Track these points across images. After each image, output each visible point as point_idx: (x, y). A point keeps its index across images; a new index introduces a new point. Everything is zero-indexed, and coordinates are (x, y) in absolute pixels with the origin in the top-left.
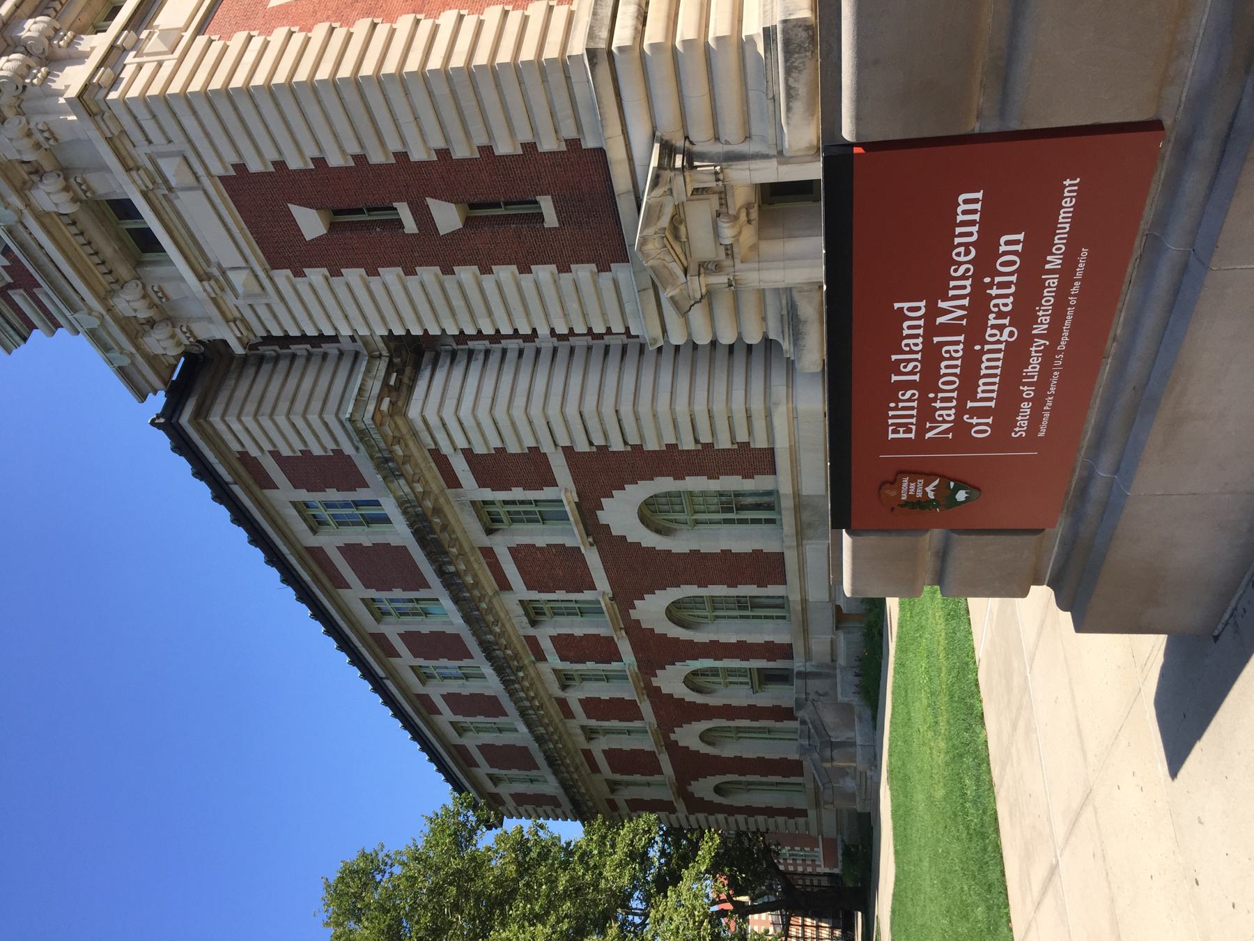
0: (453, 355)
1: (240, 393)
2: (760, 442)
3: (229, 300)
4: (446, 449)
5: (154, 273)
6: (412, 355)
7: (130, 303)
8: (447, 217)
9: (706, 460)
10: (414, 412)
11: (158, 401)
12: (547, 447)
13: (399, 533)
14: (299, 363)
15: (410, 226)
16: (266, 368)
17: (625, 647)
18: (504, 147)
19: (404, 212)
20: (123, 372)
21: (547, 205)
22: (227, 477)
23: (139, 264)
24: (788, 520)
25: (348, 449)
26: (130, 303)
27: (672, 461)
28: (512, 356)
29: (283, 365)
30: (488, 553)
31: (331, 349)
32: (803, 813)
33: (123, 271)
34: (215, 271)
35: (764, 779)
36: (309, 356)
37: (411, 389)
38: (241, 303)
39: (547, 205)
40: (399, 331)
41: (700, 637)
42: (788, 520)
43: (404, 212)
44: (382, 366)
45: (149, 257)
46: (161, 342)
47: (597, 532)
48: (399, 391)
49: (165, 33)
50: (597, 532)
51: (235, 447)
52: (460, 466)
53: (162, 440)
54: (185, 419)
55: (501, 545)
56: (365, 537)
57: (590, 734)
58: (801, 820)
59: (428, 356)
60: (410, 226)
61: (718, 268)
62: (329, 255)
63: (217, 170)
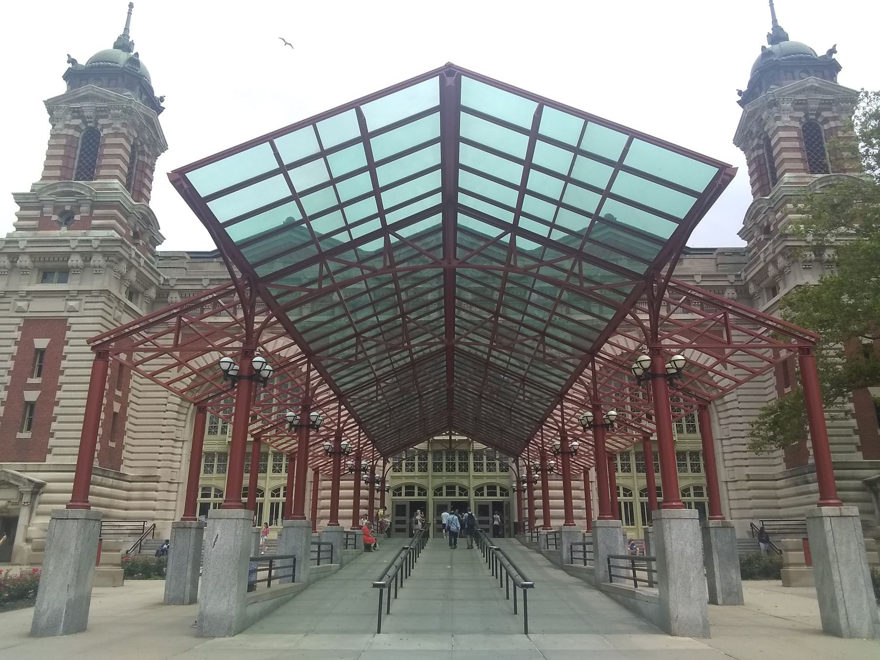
3: (15, 297)
5: (35, 276)
8: (31, 396)
15: (30, 381)
18: (54, 425)
19: (38, 380)
21: (26, 435)
23: (40, 270)
33: (38, 264)
34: (28, 298)
39: (26, 435)
43: (38, 380)
45: (41, 275)
49: (120, 317)
60: (30, 381)
62: (24, 344)
63: (71, 320)
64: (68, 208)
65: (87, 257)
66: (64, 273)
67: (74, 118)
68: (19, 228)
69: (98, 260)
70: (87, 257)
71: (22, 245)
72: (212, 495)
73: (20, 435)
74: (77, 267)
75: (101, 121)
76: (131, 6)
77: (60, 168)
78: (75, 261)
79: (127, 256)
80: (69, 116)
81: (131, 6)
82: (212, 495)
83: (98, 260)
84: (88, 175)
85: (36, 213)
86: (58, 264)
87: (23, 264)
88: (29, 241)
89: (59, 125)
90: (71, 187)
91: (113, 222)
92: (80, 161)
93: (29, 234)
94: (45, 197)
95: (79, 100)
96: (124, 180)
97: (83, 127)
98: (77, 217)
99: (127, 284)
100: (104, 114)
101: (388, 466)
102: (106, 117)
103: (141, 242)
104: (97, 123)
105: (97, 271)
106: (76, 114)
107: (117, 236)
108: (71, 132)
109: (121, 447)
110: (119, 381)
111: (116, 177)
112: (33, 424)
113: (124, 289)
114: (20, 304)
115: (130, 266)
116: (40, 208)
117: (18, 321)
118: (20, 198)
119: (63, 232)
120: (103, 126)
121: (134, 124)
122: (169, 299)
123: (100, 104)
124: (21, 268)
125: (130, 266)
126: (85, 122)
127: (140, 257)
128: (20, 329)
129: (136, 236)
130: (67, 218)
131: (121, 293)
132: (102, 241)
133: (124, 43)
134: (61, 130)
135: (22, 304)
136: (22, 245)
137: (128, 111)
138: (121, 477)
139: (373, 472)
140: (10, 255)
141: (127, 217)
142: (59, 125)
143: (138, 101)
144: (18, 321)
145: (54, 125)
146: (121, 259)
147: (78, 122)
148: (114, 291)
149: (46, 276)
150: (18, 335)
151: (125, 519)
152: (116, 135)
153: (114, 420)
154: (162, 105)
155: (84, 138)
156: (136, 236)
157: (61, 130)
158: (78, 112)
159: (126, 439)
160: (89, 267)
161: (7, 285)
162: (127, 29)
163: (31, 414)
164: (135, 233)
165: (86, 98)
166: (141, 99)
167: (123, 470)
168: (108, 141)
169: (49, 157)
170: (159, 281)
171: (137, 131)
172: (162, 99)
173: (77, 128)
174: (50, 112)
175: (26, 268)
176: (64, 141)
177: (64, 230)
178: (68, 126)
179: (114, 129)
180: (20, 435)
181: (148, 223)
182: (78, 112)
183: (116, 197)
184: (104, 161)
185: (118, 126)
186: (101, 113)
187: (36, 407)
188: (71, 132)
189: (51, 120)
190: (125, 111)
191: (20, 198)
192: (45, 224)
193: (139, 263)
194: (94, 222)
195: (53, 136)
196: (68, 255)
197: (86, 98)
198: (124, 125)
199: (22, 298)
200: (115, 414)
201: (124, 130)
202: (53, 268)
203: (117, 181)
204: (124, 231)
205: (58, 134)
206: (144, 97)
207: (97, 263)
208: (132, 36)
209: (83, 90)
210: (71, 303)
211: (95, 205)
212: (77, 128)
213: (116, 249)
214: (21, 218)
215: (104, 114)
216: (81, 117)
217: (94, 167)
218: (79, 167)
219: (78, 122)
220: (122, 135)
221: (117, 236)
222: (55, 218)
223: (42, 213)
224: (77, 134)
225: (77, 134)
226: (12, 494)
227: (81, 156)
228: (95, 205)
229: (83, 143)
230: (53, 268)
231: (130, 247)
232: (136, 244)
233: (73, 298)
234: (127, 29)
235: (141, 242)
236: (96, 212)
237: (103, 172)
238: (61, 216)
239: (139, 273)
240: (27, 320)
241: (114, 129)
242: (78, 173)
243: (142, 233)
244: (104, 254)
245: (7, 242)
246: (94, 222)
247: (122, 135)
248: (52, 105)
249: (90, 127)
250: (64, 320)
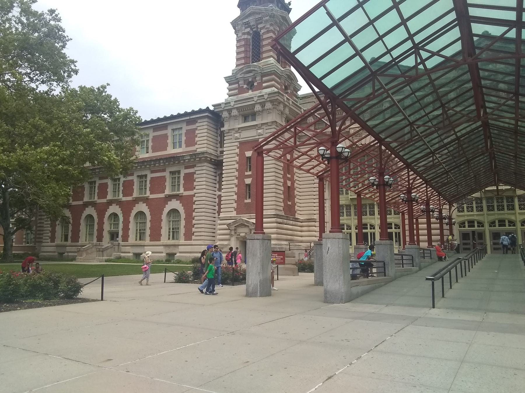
0: (216, 173)
1: (212, 125)
2: (193, 237)
3: (233, 132)
4: (196, 169)
5: (241, 119)
6: (218, 165)
7: (235, 112)
9: (189, 225)
10: (206, 164)
11: (212, 108)
12: (195, 191)
13: (171, 151)
14: (215, 138)
15: (246, 173)
16: (215, 131)
17: (129, 198)
19: (249, 173)
20: (219, 105)
22: (191, 117)
23: (242, 116)
24: (171, 242)
25: (197, 146)
26: (235, 112)
27: (189, 218)
28: (215, 185)
29: (216, 135)
30: (164, 170)
31: (219, 145)
32: (53, 240)
33: (241, 113)
34: (240, 131)
35: (70, 231)
36: (217, 140)
37: (210, 163)
38: (232, 134)
40: (224, 164)
41: (132, 219)
42: (171, 242)
43: (249, 173)
44: (216, 159)
46: (225, 115)
47: (170, 198)
48: (210, 162)
50: (170, 198)
51: (199, 121)
52: (191, 170)
53: (204, 108)
54: (207, 114)
55: (167, 174)
56: (170, 141)
57: (92, 183)
58: (49, 241)
59: (216, 167)
60: (246, 173)
61: (235, 233)
62: (241, 155)
64: (250, 80)
65: (263, 104)
66: (253, 115)
67: (246, 28)
68: (230, 96)
69: (268, 105)
70: (263, 104)
71: (232, 104)
72: (345, 229)
73: (246, 201)
74: (259, 111)
75: (260, 26)
77: (244, 58)
78: (258, 108)
79: (282, 100)
80: (244, 27)
82: (345, 229)
83: (268, 105)
84: (258, 59)
85: (236, 85)
86: (250, 111)
87: (234, 114)
88: (235, 102)
90: (250, 67)
91: (273, 82)
92: (253, 52)
93: (234, 98)
94: (239, 76)
95: (247, 17)
96: (276, 57)
97: (251, 32)
98: (255, 84)
99: (285, 116)
100: (260, 21)
101: (453, 208)
102: (261, 23)
103: (289, 91)
104: (257, 28)
105: (269, 111)
106: (247, 26)
107: (276, 90)
108: (246, 36)
109: (294, 204)
110: (288, 169)
111: (271, 56)
112: (251, 195)
113: (284, 119)
114: (236, 135)
115: (285, 106)
116: (238, 83)
117: (237, 144)
118: (228, 80)
119: (250, 94)
120: (261, 29)
121: (276, 23)
122: (308, 121)
123: (257, 16)
124: (234, 116)
125: (285, 106)
126: (252, 29)
127: (289, 100)
128: (238, 148)
129: (286, 88)
130: (251, 86)
131: (282, 122)
132: (269, 94)
134: (241, 36)
135: (237, 135)
136: (232, 104)
137: (272, 16)
138: (296, 220)
139: (440, 212)
140: (228, 110)
141: (280, 79)
142: (240, 34)
143: (277, 9)
144: (237, 144)
145: (237, 35)
146: (280, 102)
147: (248, 30)
148: (279, 121)
149: (246, 118)
150: (237, 151)
151: (302, 242)
152: (268, 32)
153: (289, 190)
154: (290, 7)
155: (253, 38)
156: (286, 88)
157: (241, 36)
158: (248, 24)
159: (296, 200)
160: (265, 110)
161: (229, 126)
163: (249, 190)
164: (286, 87)
165: (250, 15)
166: (278, 7)
167: (297, 216)
169: (238, 53)
170: (301, 112)
171: (278, 26)
172: (290, 4)
173: (248, 33)
174: (234, 28)
175: (236, 116)
176: (243, 43)
177: (250, 92)
178: (244, 34)
179: (266, 29)
180: (246, 201)
181: (292, 79)
182: (248, 24)
183: (272, 68)
185: (268, 26)
186: (259, 21)
187: (251, 186)
188: (246, 36)
189: (236, 33)
190: (270, 17)
191: (228, 80)
192: (241, 91)
193: (289, 103)
194: (264, 85)
195: (238, 41)
196: (254, 105)
197: (250, 15)
198: (271, 25)
199: (237, 132)
200: (289, 187)
201: (272, 28)
202: (248, 114)
203: (272, 59)
204: (279, 86)
205: (240, 40)
206: (280, 5)
207: (268, 107)
209: (248, 11)
210: (259, 131)
211: (263, 75)
212: (248, 33)
213: (276, 98)
214: (230, 90)
215: (260, 21)
216: (250, 26)
217: (260, 54)
218: (253, 55)
219: (248, 30)
220: (271, 31)
221: (276, 90)
222: (245, 86)
223: (239, 85)
224: (249, 37)
225: (249, 37)
226: (246, 230)
227: (253, 49)
228: (263, 75)
229: (253, 41)
230: (248, 114)
231: (283, 95)
232: (287, 93)
233: (260, 128)
235: (289, 91)
236: (264, 79)
237: (264, 55)
238: (247, 85)
239: (290, 109)
240: (241, 143)
241: (266, 29)
242: (252, 59)
243: (289, 86)
244: (271, 101)
245: (226, 104)
246: (264, 85)
247: (271, 31)
249: (255, 31)
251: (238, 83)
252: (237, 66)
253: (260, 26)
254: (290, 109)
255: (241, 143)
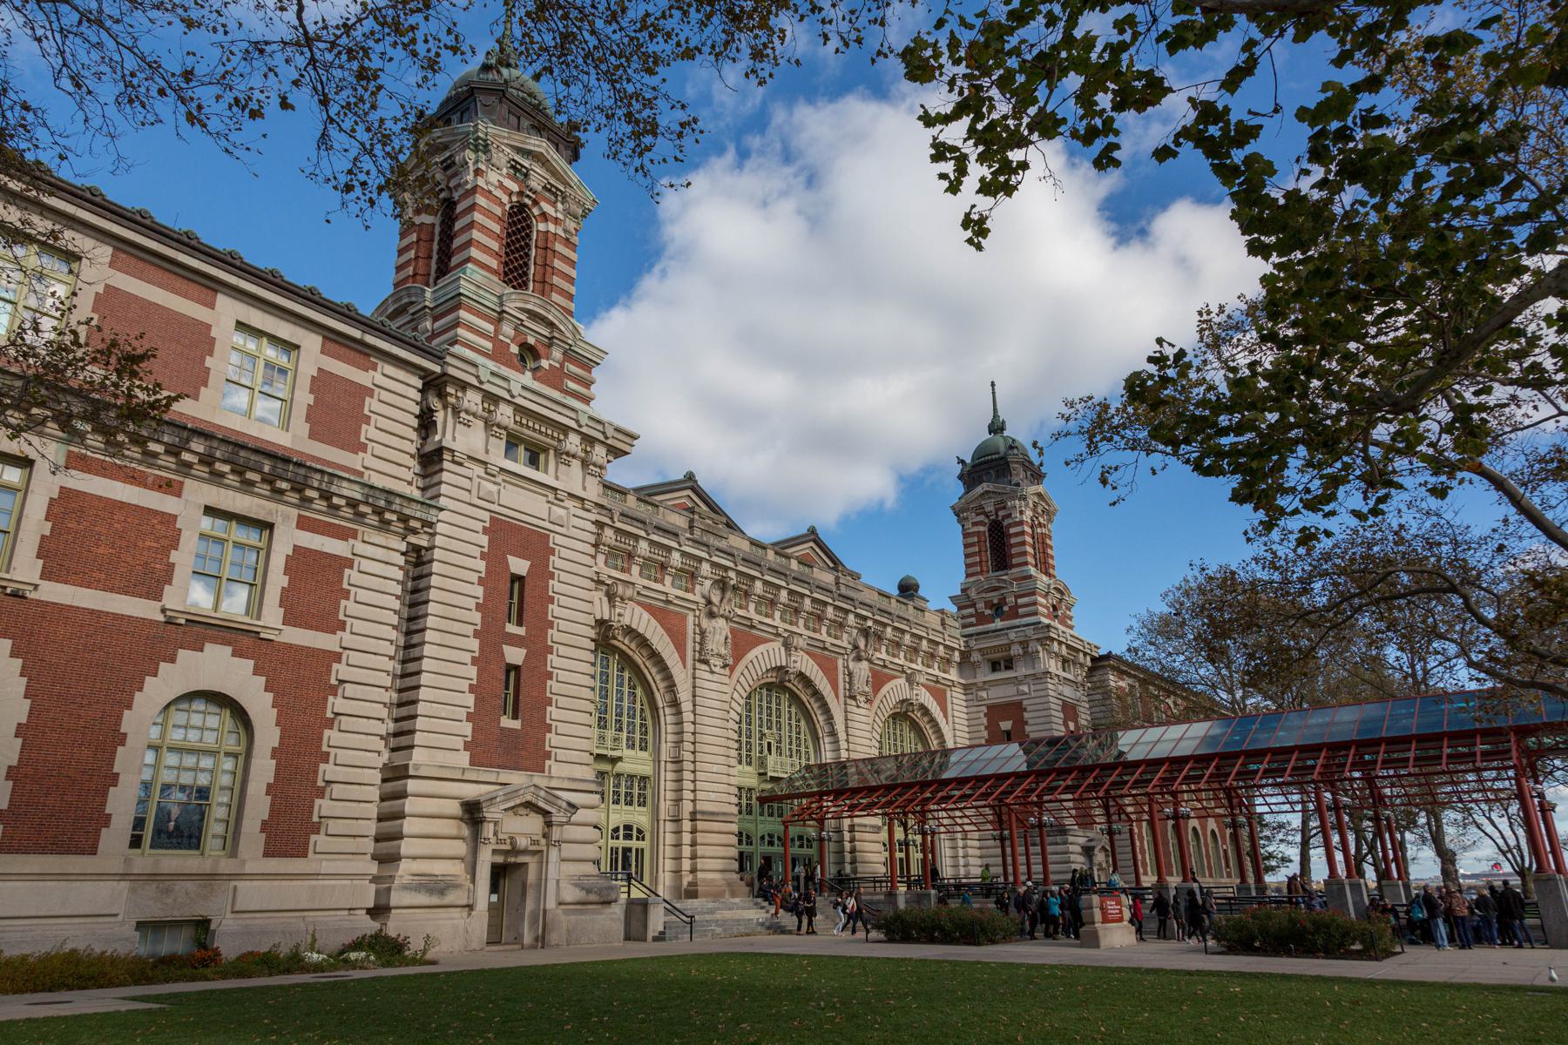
5: (986, 668)
76: (993, 384)
81: (993, 384)
85: (972, 610)
89: (968, 525)
98: (1006, 608)
115: (1060, 643)
116: (974, 605)
119: (998, 624)
125: (1060, 643)
133: (996, 427)
135: (984, 694)
142: (968, 525)
147: (982, 518)
149: (995, 666)
162: (995, 410)
168: (1012, 531)
178: (975, 524)
184: (1014, 551)
192: (981, 619)
195: (966, 535)
196: (1009, 646)
208: (1002, 416)
222: (988, 612)
234: (995, 410)
236: (1020, 601)
239: (1068, 647)
240: (989, 707)
246: (1021, 611)
248: (958, 512)
250: (1020, 703)
251: (974, 605)
252: (968, 576)
253: (1001, 513)
254: (1068, 647)
255: (989, 707)
